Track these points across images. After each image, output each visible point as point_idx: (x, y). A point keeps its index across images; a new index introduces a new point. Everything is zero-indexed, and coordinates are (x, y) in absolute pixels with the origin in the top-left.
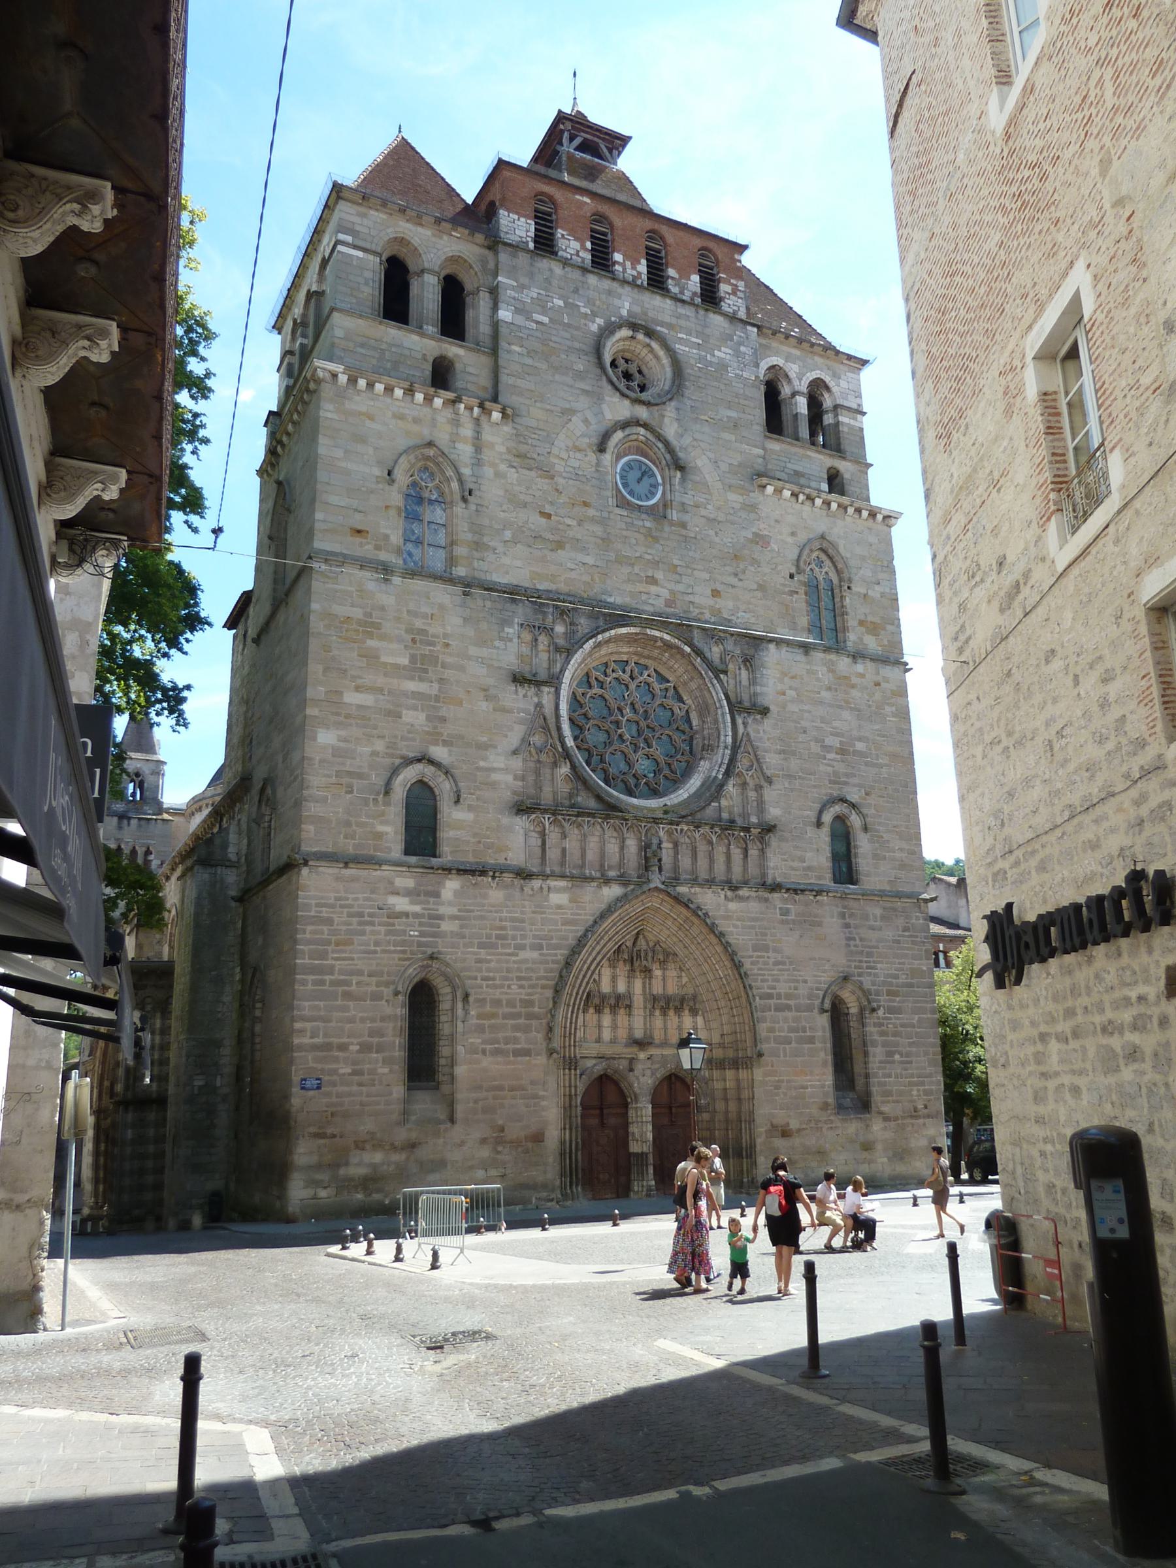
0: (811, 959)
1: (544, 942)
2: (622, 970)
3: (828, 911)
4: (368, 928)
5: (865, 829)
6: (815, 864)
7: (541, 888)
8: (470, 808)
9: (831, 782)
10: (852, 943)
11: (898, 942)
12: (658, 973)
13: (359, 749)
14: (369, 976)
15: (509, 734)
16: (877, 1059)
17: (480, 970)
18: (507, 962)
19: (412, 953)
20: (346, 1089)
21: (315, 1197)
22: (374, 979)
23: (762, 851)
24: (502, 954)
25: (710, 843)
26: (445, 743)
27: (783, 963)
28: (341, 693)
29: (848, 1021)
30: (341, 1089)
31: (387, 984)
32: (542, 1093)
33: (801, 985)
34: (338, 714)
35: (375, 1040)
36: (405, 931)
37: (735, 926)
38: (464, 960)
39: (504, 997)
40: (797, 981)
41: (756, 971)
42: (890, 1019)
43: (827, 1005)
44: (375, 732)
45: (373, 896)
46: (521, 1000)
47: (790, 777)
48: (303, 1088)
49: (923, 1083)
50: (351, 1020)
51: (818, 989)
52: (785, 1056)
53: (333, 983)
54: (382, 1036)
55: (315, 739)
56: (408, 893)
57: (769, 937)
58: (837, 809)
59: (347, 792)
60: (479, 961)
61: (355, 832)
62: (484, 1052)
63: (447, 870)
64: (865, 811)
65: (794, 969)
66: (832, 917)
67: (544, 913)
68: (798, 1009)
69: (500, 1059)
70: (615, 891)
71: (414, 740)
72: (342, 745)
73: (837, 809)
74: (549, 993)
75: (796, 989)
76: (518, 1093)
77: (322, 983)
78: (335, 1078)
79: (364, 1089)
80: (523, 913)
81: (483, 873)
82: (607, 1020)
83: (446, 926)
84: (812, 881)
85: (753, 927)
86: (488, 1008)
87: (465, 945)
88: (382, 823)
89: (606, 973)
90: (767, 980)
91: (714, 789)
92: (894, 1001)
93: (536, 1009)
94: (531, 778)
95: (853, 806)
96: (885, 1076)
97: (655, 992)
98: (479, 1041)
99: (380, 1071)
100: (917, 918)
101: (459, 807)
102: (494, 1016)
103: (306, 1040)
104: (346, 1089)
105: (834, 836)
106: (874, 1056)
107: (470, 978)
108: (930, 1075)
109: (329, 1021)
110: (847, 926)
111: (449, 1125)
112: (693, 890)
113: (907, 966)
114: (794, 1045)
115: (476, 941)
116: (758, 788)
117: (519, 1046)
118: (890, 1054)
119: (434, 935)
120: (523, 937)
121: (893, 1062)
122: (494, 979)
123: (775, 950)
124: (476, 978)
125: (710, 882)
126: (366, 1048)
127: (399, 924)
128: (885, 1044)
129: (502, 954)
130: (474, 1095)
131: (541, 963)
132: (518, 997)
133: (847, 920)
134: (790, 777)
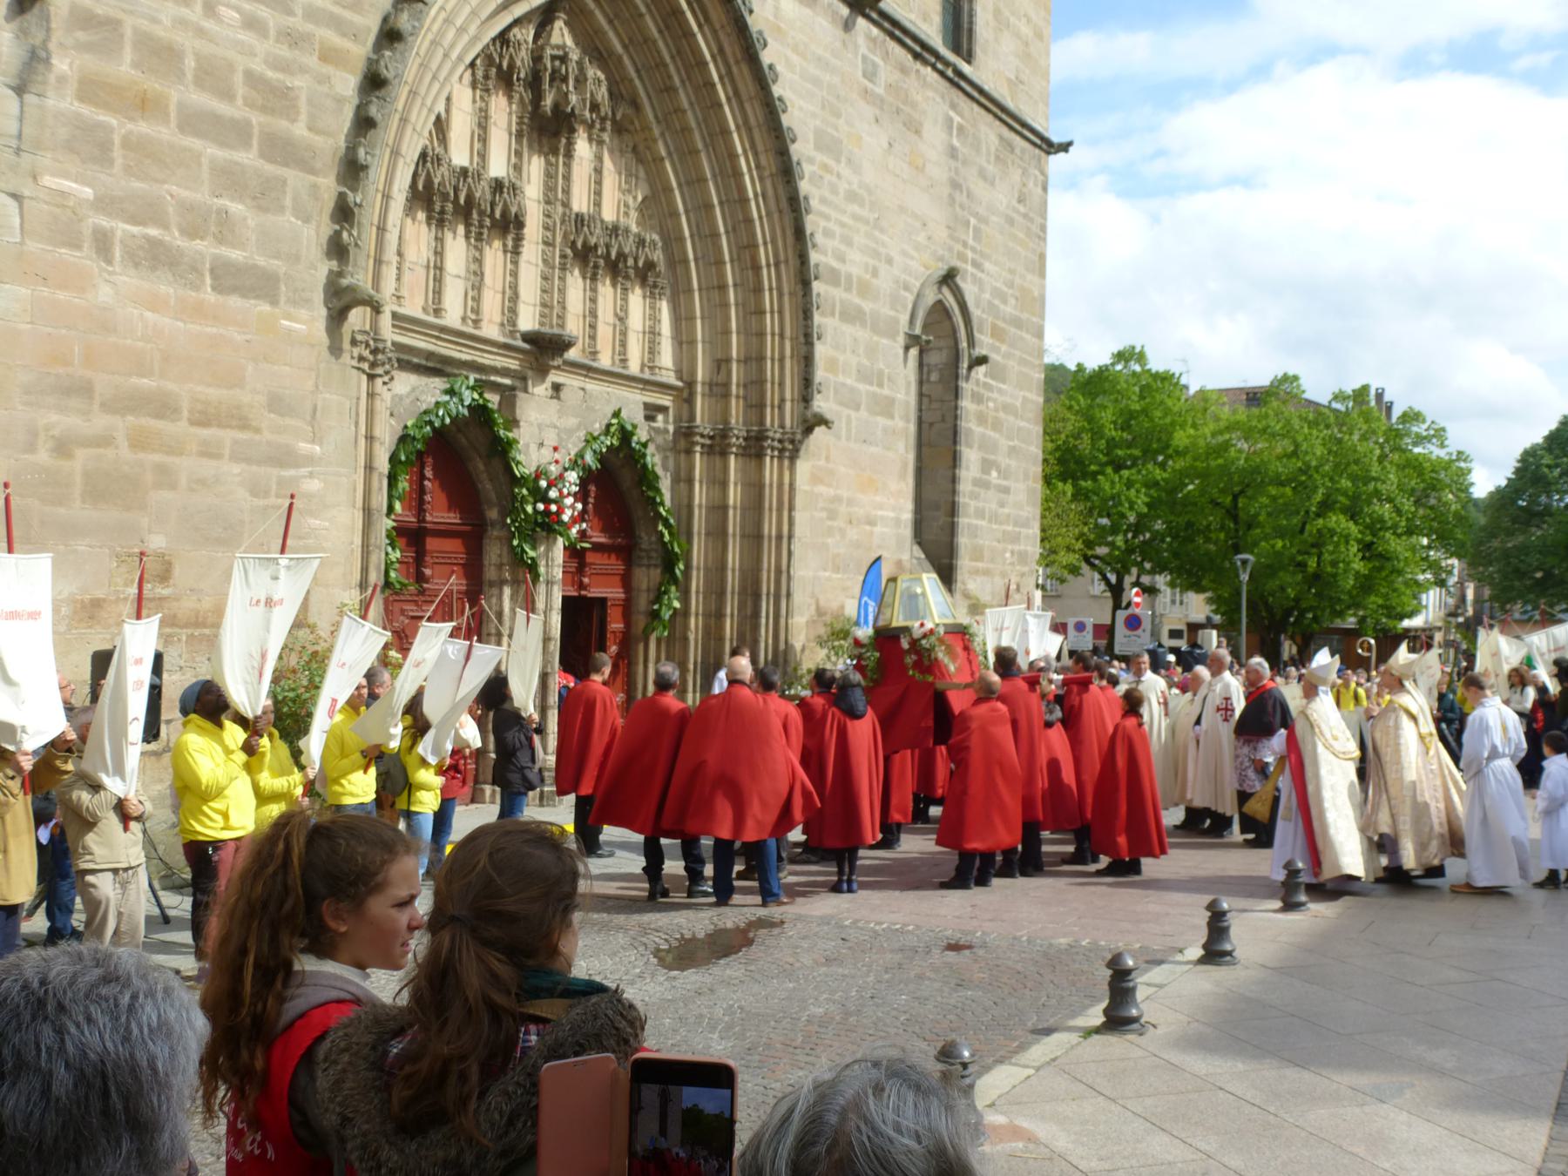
2: (502, 111)
12: (583, 147)
32: (304, 447)
33: (883, 268)
39: (187, 42)
46: (251, 78)
51: (907, 288)
52: (848, 439)
57: (841, 122)
62: (103, 243)
69: (166, 288)
74: (348, 84)
76: (228, 436)
82: (457, 247)
85: (816, 82)
86: (124, 68)
89: (464, 98)
93: (300, 130)
98: (88, 192)
117: (235, 255)
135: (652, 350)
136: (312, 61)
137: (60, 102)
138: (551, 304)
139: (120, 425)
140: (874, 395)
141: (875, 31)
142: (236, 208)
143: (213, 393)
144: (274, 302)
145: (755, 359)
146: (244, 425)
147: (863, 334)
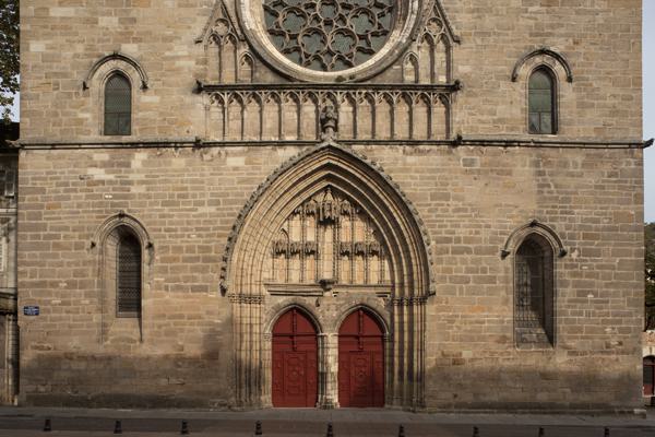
0: (497, 206)
1: (221, 199)
2: (311, 222)
3: (521, 163)
4: (72, 194)
5: (570, 79)
6: (509, 116)
7: (219, 153)
8: (156, 92)
9: (531, 35)
10: (546, 189)
11: (603, 188)
12: (345, 222)
13: (64, 54)
14: (74, 231)
15: (193, 26)
16: (566, 298)
17: (164, 223)
18: (188, 216)
19: (107, 212)
20: (58, 315)
21: (36, 391)
22: (77, 234)
23: (448, 108)
24: (182, 210)
25: (390, 102)
26: (136, 40)
27: (466, 210)
28: (48, 9)
29: (543, 264)
30: (53, 315)
31: (88, 237)
34: (46, 27)
35: (78, 279)
36: (101, 195)
37: (412, 178)
38: (150, 216)
40: (480, 226)
41: (434, 218)
42: (586, 261)
43: (512, 247)
44: (76, 38)
45: (76, 169)
46: (199, 247)
47: (484, 34)
48: (26, 314)
49: (620, 322)
50: (61, 265)
51: (501, 233)
53: (45, 237)
54: (84, 276)
55: (28, 49)
56: (104, 165)
57: (450, 186)
58: (539, 60)
59: (54, 89)
60: (163, 216)
61: (61, 120)
62: (166, 288)
63: (135, 145)
64: (570, 61)
65: (476, 216)
66: (524, 166)
67: (221, 174)
68: (478, 251)
69: (180, 294)
70: (292, 152)
71: (108, 40)
72: (48, 51)
73: (539, 60)
74: (224, 241)
75: (477, 233)
77: (38, 237)
78: (49, 307)
79: (71, 315)
80: (202, 175)
81: (166, 144)
83: (134, 190)
84: (503, 132)
85: (434, 178)
86: (170, 254)
87: (151, 204)
88: (82, 111)
90: (446, 226)
91: (402, 53)
92: (592, 244)
93: (213, 254)
94: (214, 62)
95: (556, 56)
96: (574, 314)
97: (344, 240)
99: (83, 302)
100: (628, 163)
101: (148, 91)
102: (175, 260)
103: (27, 280)
104: (58, 315)
105: (533, 89)
106: (563, 295)
107: (155, 230)
108: (630, 314)
109: (44, 265)
110: (541, 173)
111: (138, 343)
112: (369, 147)
113: (610, 210)
114: (471, 284)
115: (160, 200)
116: (448, 49)
117: (196, 284)
119: (125, 197)
120: (203, 195)
121: (586, 301)
122: (176, 230)
123: (456, 198)
124: (160, 230)
125: (391, 142)
126: (71, 285)
127: (96, 190)
128: (576, 285)
129: (182, 210)
130: (157, 322)
131: (218, 216)
132: (196, 244)
133: (542, 169)
134: (484, 34)
135: (382, 275)
136: (216, 239)
137: (157, 264)
138: (335, 271)
139: (172, 321)
140: (479, 278)
141: (472, 148)
142: (195, 274)
143: (192, 313)
144: (206, 291)
145: (411, 274)
146: (200, 318)
147: (469, 257)
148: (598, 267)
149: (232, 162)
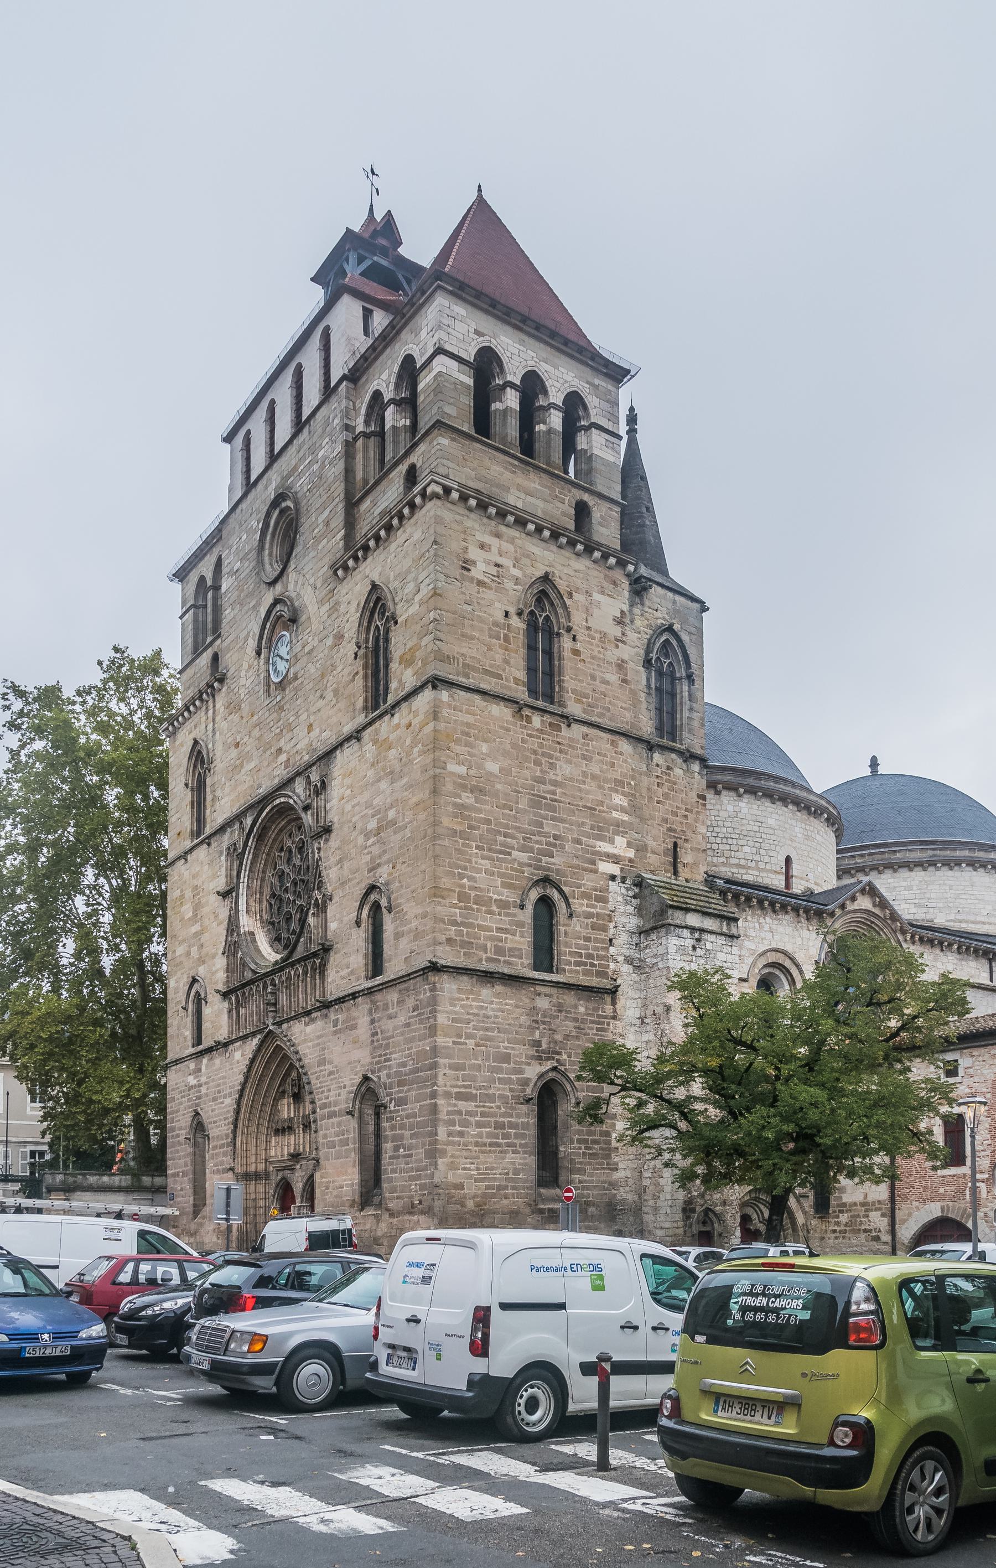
10: (375, 1038)
40: (340, 1087)
49: (419, 1177)
114: (337, 1148)
118: (396, 1149)
147: (335, 1120)
148: (408, 1117)
149: (238, 1055)
